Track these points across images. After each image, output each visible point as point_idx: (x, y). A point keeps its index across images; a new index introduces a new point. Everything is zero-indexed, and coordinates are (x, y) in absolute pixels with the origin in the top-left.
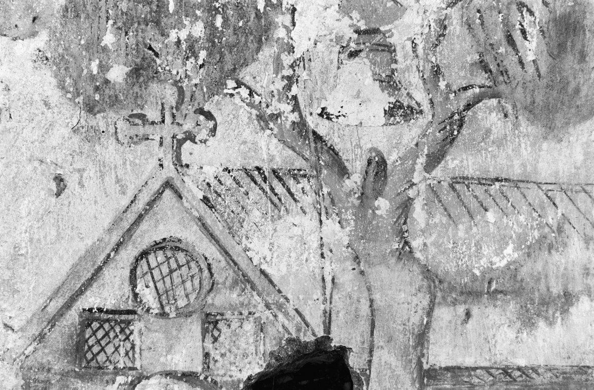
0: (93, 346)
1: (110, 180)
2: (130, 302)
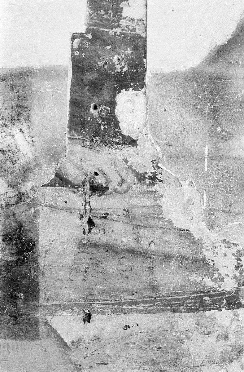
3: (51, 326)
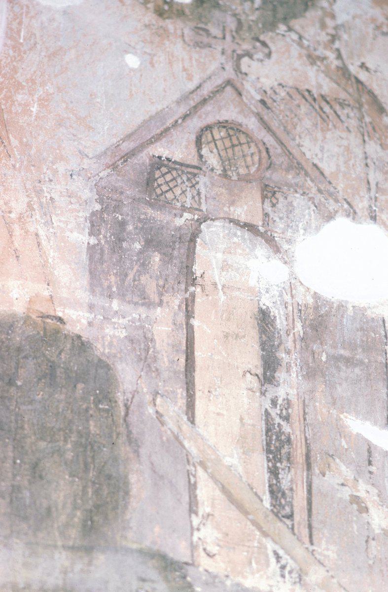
0: (162, 185)
1: (178, 67)
2: (196, 160)
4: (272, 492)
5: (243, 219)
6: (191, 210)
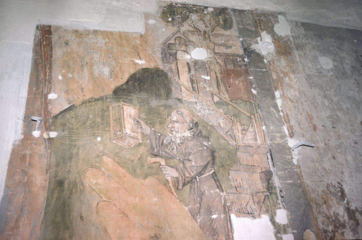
3: (58, 114)
4: (192, 88)
5: (183, 50)
6: (175, 50)
